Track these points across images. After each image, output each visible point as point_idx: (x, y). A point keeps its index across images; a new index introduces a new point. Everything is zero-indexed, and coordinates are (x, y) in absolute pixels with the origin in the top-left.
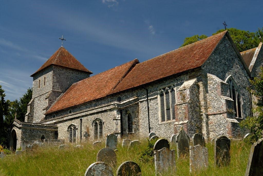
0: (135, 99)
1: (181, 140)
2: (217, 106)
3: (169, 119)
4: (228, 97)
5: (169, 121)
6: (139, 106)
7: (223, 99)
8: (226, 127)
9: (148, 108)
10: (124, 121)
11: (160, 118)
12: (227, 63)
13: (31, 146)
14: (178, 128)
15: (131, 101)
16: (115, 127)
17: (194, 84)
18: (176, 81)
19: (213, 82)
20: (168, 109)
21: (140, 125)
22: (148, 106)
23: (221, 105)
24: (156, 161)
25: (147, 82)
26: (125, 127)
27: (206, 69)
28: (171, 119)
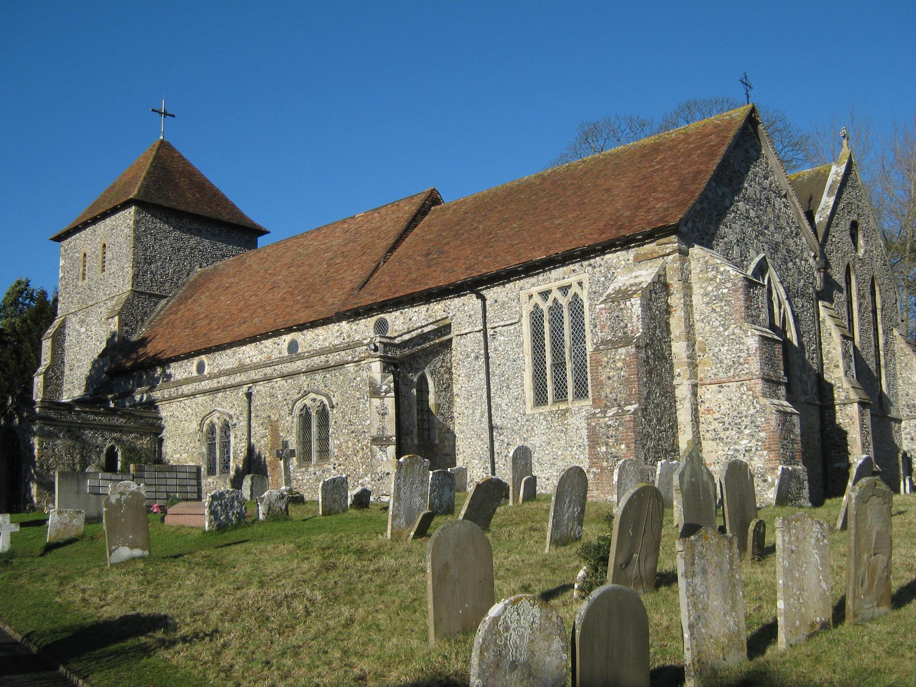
0: (441, 328)
1: (692, 484)
2: (729, 357)
3: (561, 395)
4: (764, 327)
5: (563, 406)
6: (454, 353)
7: (749, 334)
8: (759, 429)
9: (487, 357)
10: (406, 402)
11: (529, 394)
12: (752, 214)
13: (123, 499)
14: (602, 430)
15: (429, 332)
16: (377, 425)
17: (654, 283)
18: (590, 268)
19: (715, 277)
20: (559, 365)
21: (455, 415)
22: (487, 354)
23: (742, 355)
24: (686, 577)
25: (484, 271)
26: (407, 423)
27: (693, 232)
28: (570, 397)
